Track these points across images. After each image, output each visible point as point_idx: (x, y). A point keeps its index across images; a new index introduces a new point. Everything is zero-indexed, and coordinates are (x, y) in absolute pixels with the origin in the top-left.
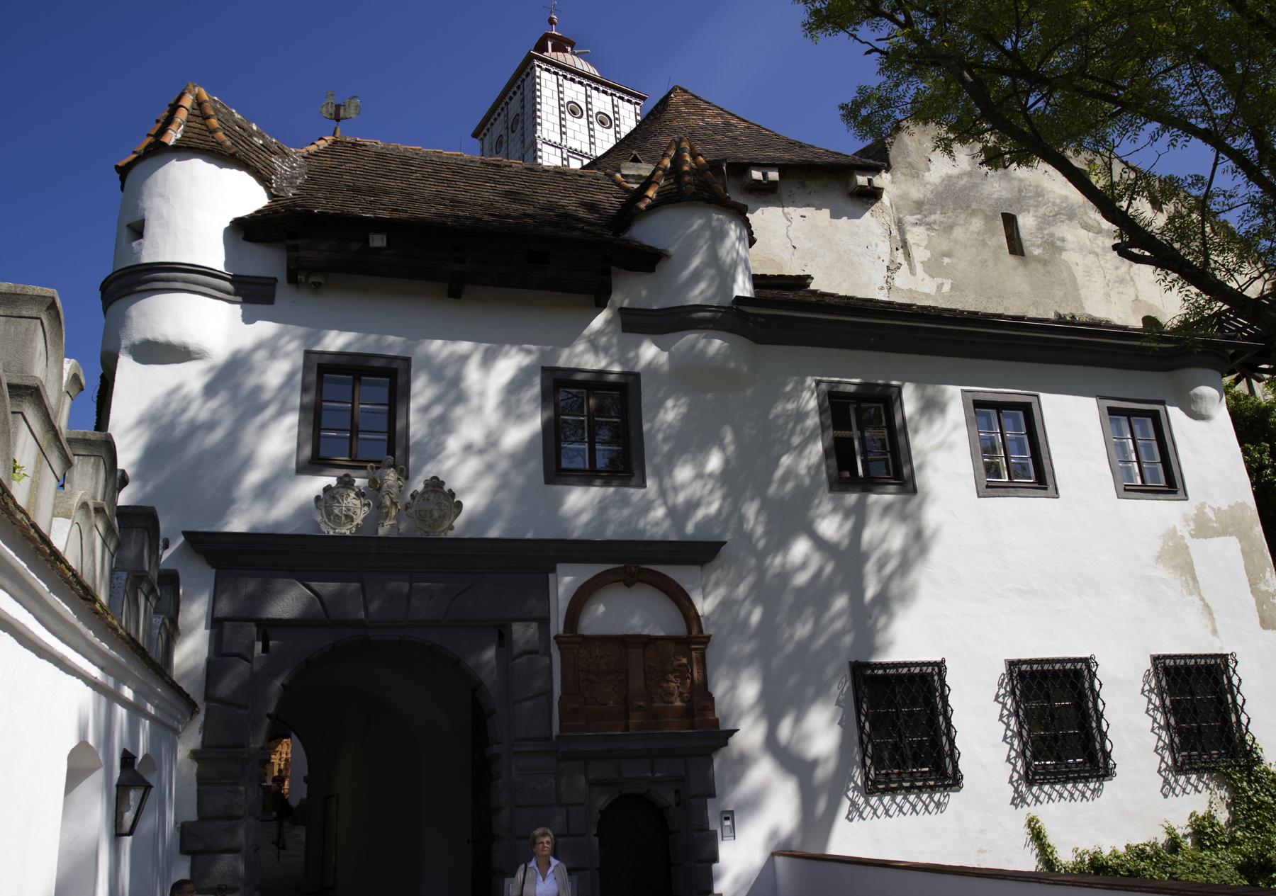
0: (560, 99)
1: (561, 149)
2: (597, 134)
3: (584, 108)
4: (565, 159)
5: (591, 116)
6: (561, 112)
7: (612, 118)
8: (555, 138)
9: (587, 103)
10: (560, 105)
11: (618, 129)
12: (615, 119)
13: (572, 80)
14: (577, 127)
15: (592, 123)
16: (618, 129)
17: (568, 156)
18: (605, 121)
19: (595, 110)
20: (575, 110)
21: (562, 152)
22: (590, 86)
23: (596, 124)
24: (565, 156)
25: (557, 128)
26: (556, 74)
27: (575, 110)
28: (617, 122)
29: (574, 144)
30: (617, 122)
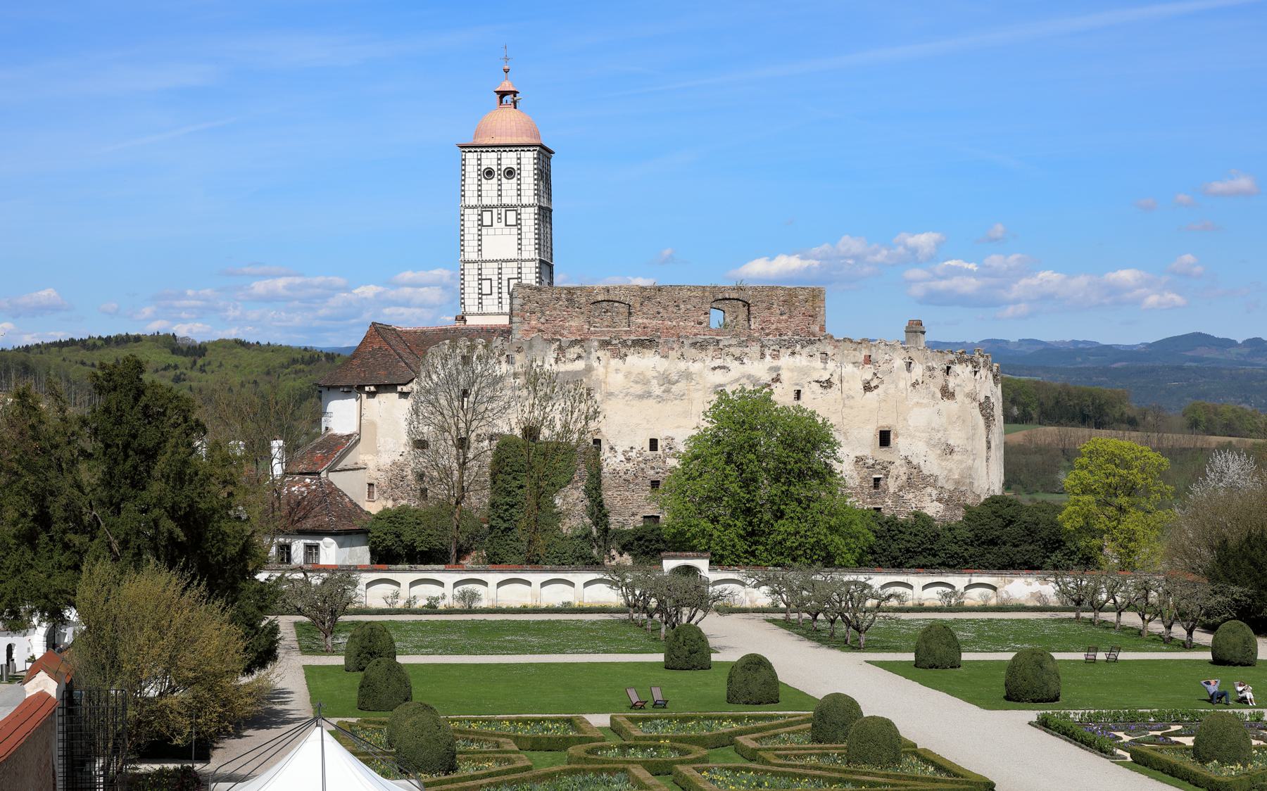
0: (479, 170)
2: (504, 187)
3: (495, 170)
6: (480, 180)
9: (499, 164)
10: (479, 175)
13: (487, 151)
14: (490, 186)
17: (482, 211)
18: (510, 173)
20: (489, 173)
22: (499, 151)
23: (504, 180)
24: (480, 212)
25: (476, 194)
26: (475, 151)
27: (489, 173)
29: (486, 201)
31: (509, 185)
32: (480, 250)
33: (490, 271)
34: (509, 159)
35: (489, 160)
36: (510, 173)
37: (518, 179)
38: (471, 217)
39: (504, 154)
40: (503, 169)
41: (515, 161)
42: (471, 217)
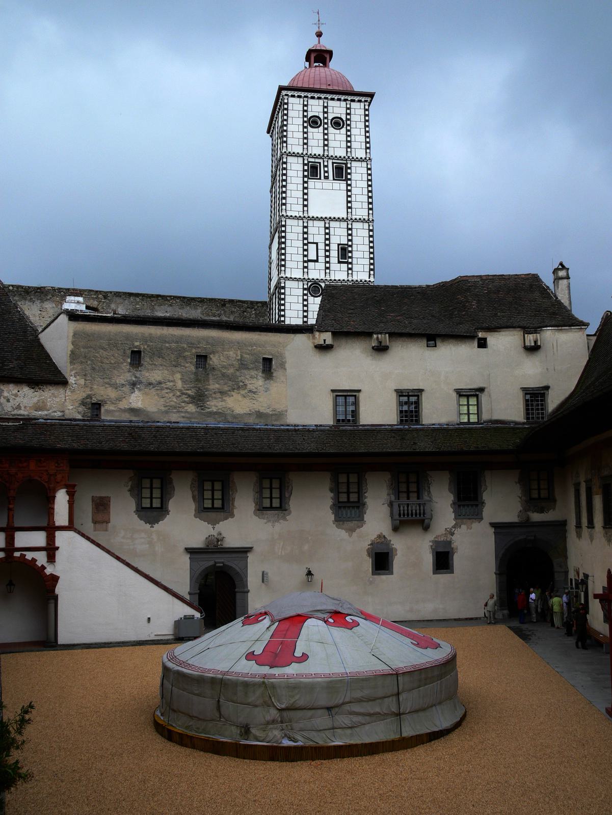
0: (304, 116)
1: (303, 157)
2: (331, 137)
4: (306, 165)
5: (327, 123)
6: (304, 127)
7: (344, 119)
8: (299, 150)
10: (304, 122)
11: (348, 128)
12: (347, 119)
14: (316, 134)
15: (327, 129)
16: (348, 128)
18: (337, 123)
19: (331, 116)
20: (314, 122)
21: (304, 160)
23: (331, 130)
26: (299, 97)
27: (314, 122)
28: (348, 122)
30: (348, 122)
31: (337, 137)
32: (306, 206)
33: (316, 232)
34: (337, 109)
35: (315, 108)
36: (337, 123)
37: (348, 131)
38: (295, 168)
39: (331, 103)
40: (330, 118)
41: (344, 111)
42: (295, 168)
